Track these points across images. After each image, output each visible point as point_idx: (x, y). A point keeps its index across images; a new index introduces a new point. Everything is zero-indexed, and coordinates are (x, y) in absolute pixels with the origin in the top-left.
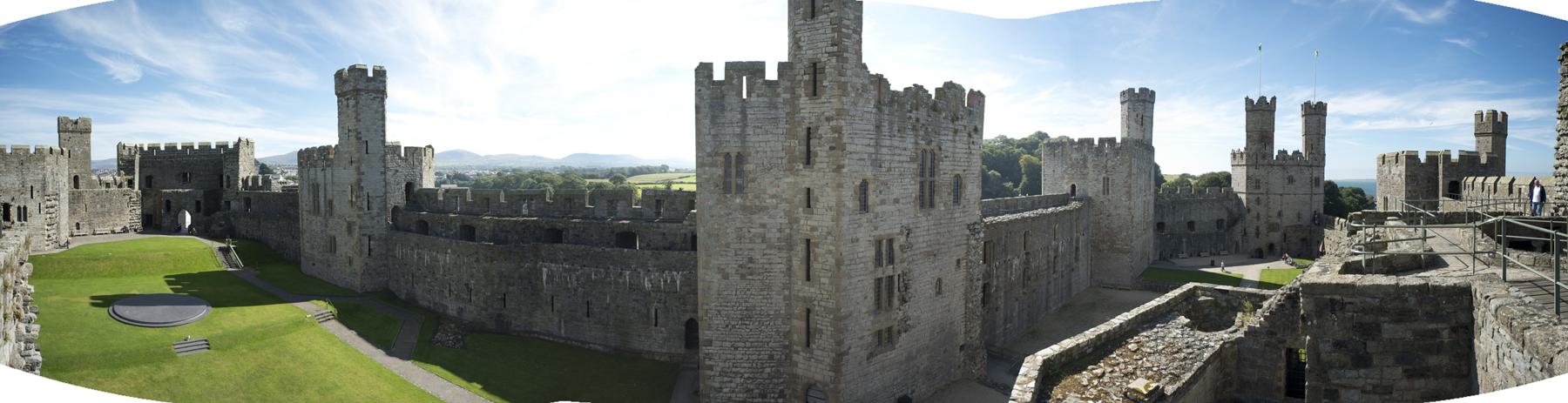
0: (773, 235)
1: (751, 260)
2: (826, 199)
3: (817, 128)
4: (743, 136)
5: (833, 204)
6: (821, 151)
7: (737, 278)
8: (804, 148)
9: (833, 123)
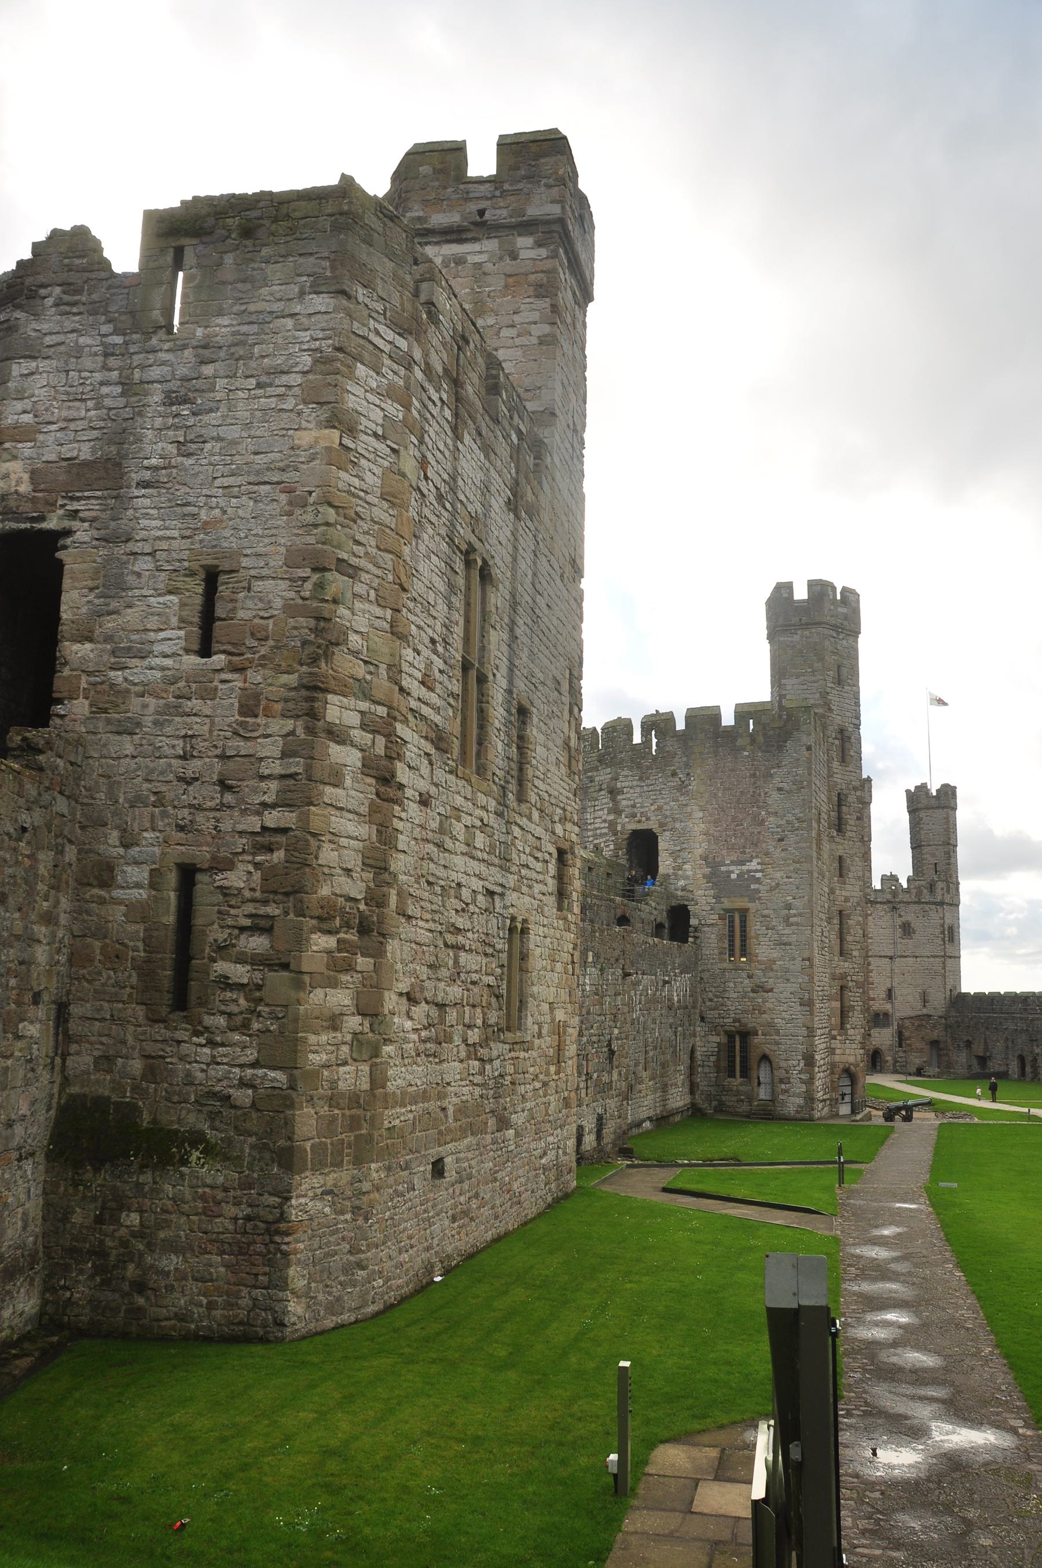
3: (846, 796)
9: (859, 793)
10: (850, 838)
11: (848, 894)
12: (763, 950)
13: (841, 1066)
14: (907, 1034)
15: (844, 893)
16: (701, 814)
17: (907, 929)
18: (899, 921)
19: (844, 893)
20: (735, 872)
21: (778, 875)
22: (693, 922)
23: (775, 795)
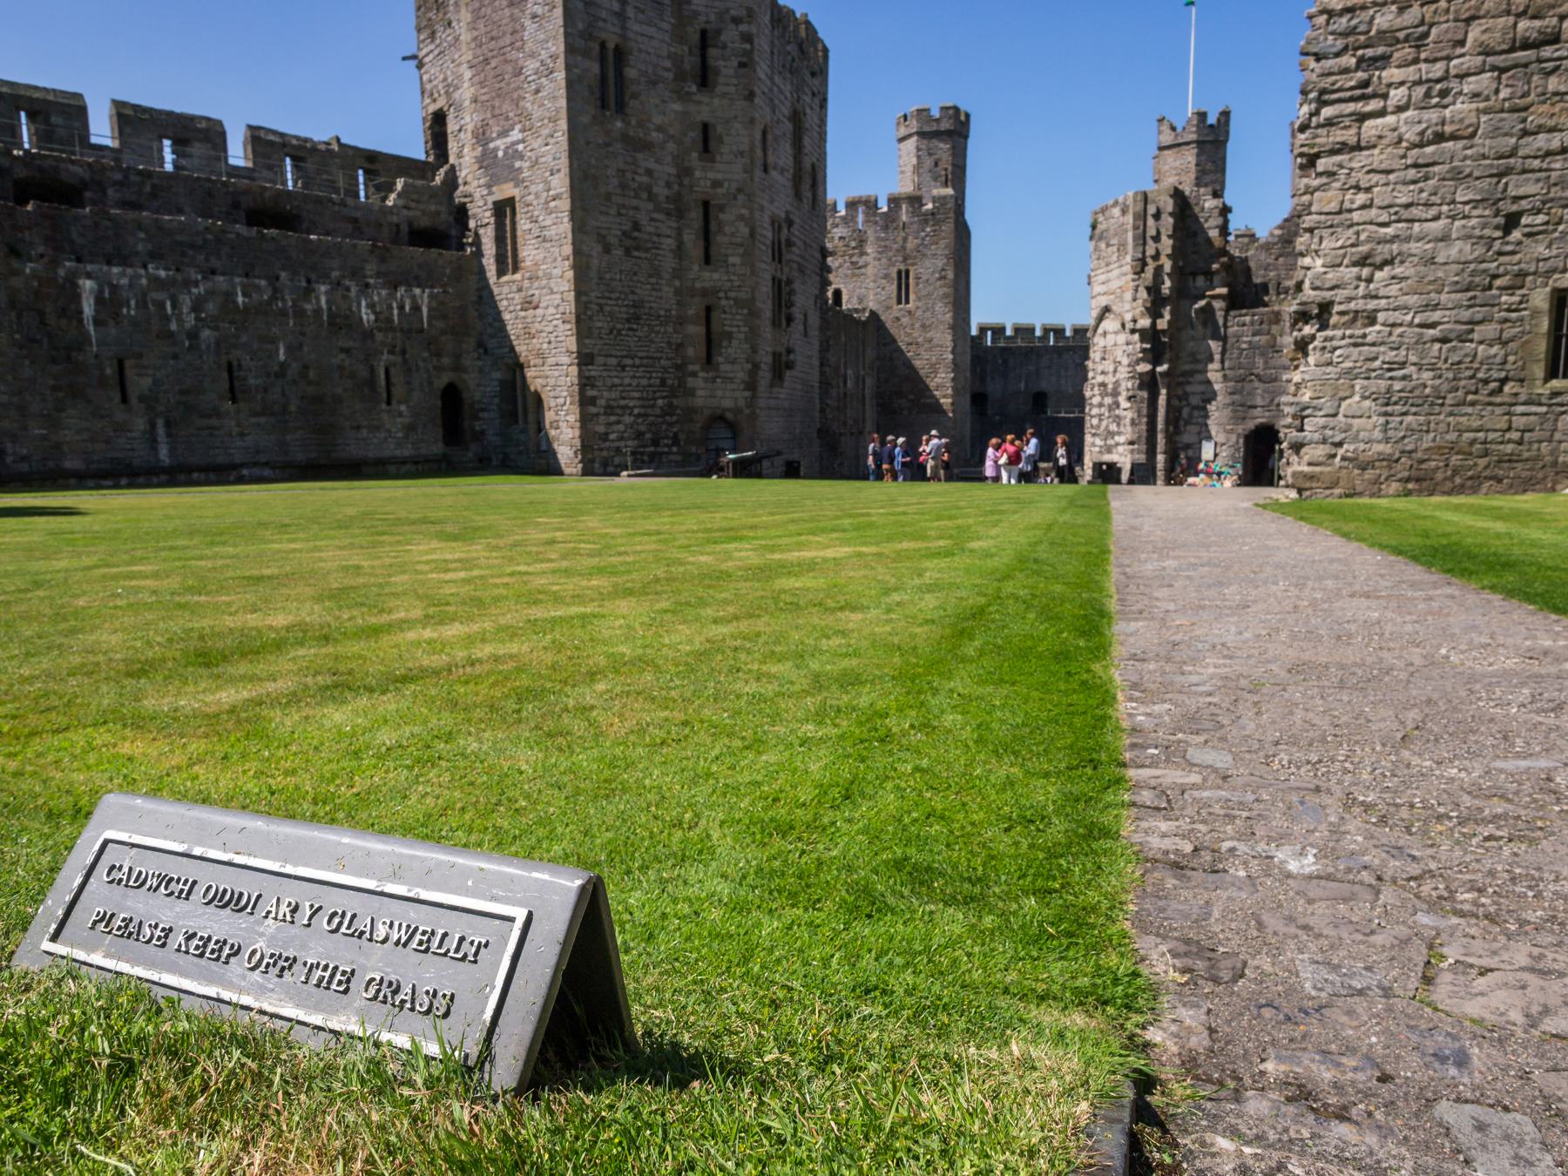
0: (661, 190)
1: (636, 226)
2: (736, 138)
3: (719, 32)
5: (745, 147)
6: (726, 68)
7: (619, 252)
8: (696, 60)
9: (744, 27)
10: (724, 95)
11: (719, 176)
13: (707, 412)
15: (711, 175)
19: (711, 175)
22: (472, 224)
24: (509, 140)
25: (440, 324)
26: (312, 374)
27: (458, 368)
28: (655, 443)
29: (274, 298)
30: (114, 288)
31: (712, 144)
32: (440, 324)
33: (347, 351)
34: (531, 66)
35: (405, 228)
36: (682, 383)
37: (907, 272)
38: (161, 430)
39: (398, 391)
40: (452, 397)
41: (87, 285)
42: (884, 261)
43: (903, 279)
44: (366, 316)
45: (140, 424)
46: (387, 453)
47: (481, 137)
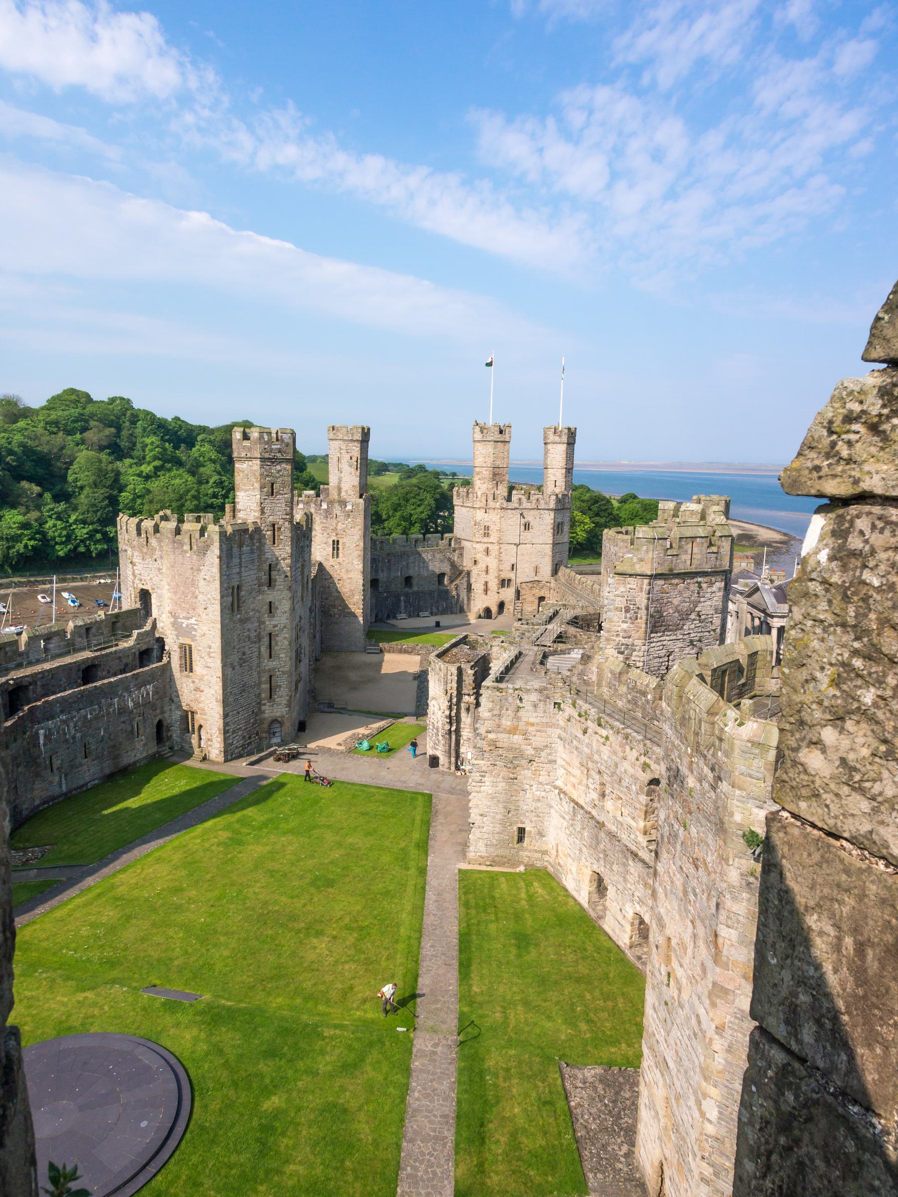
1: (244, 654)
4: (239, 573)
7: (238, 667)
8: (267, 577)
10: (279, 590)
12: (198, 667)
14: (522, 592)
16: (167, 587)
17: (527, 526)
18: (523, 521)
20: (185, 623)
21: (205, 628)
22: (166, 648)
23: (202, 582)
24: (189, 622)
25: (156, 697)
26: (112, 737)
27: (163, 712)
28: (250, 738)
29: (100, 711)
30: (50, 729)
31: (273, 610)
32: (156, 697)
33: (124, 722)
34: (201, 597)
35: (137, 653)
36: (260, 709)
37: (338, 541)
38: (63, 779)
39: (141, 731)
40: (160, 725)
41: (42, 732)
42: (325, 534)
43: (336, 545)
44: (131, 704)
45: (57, 779)
46: (137, 758)
47: (173, 614)
